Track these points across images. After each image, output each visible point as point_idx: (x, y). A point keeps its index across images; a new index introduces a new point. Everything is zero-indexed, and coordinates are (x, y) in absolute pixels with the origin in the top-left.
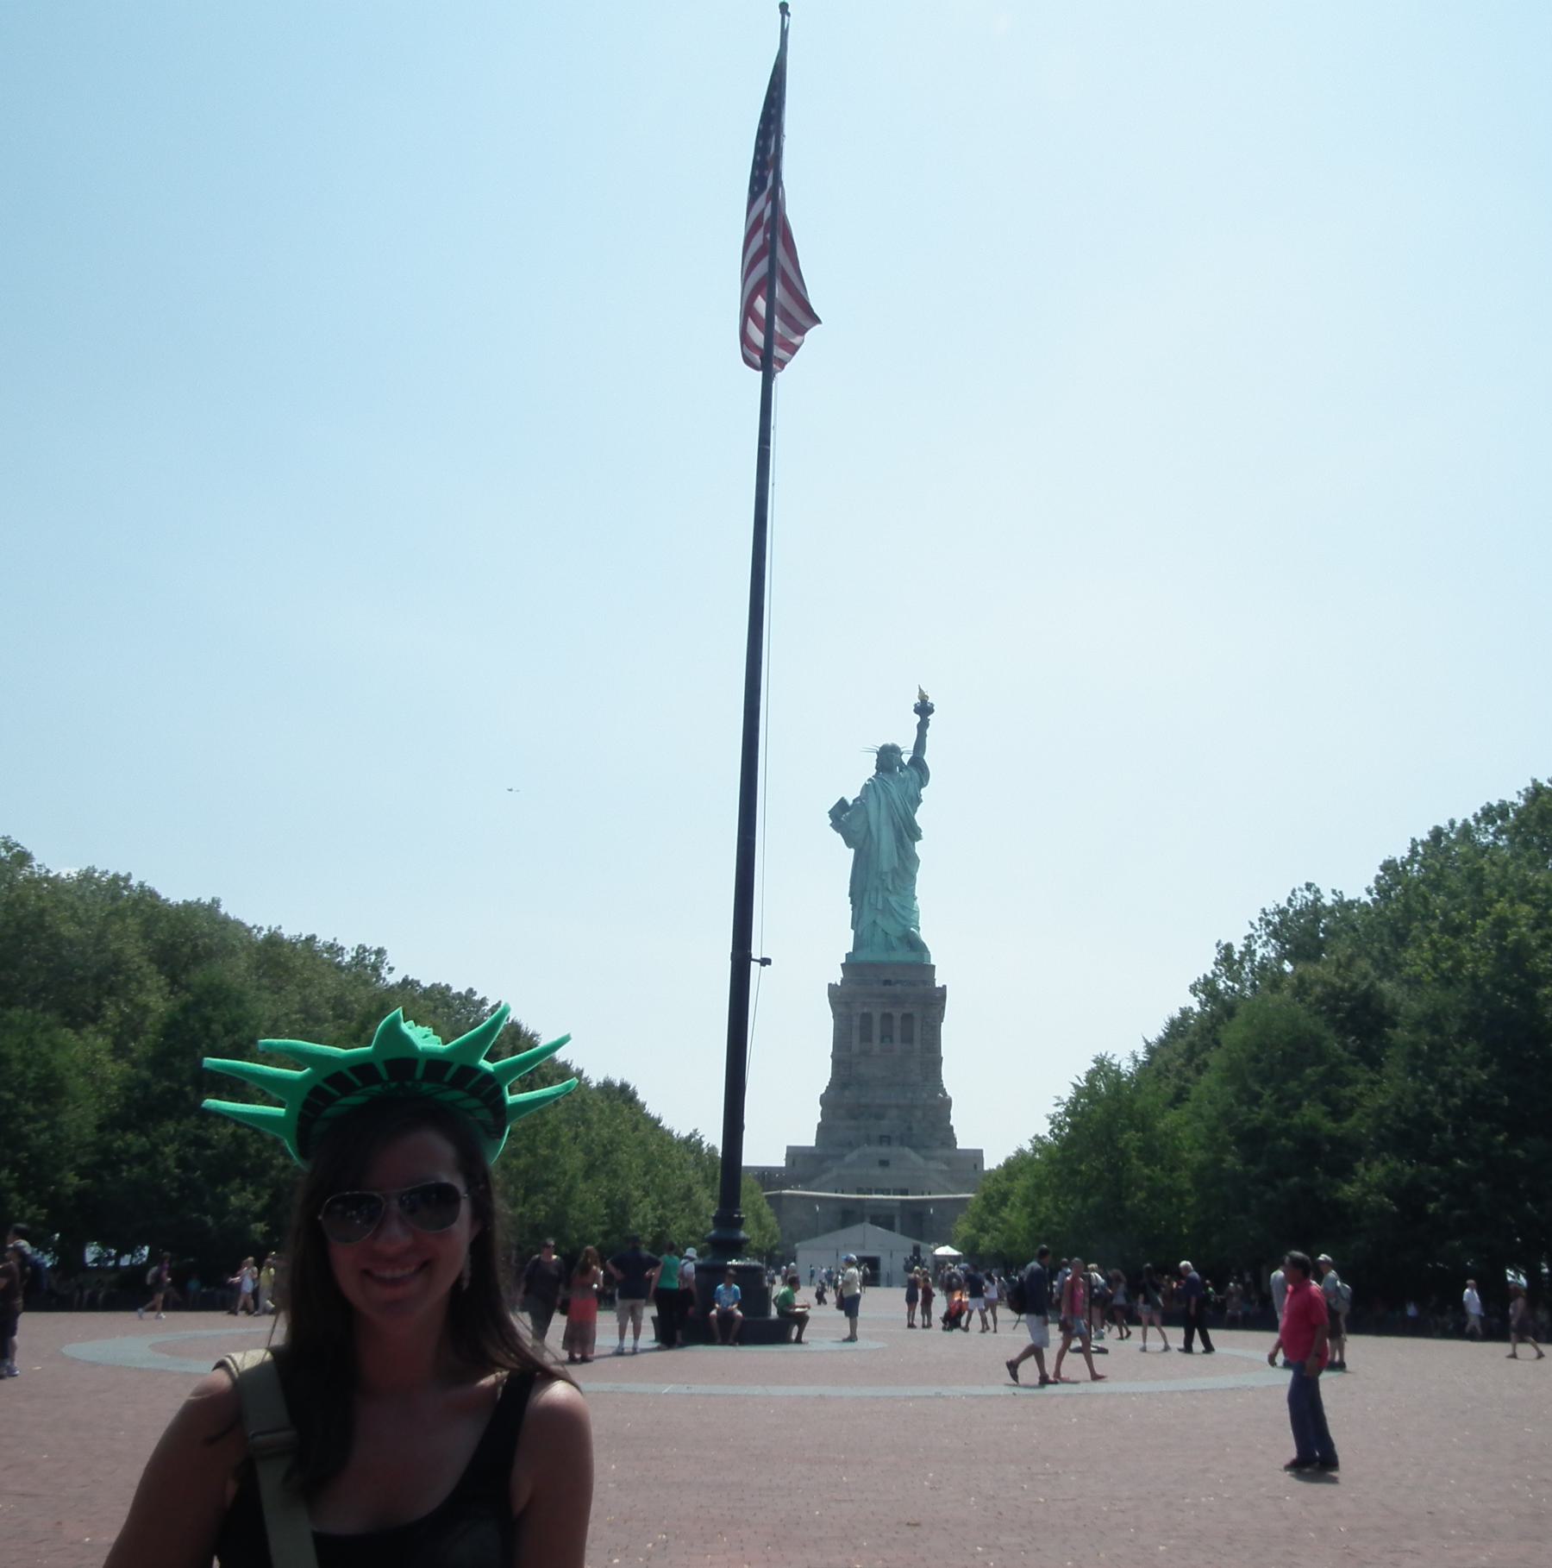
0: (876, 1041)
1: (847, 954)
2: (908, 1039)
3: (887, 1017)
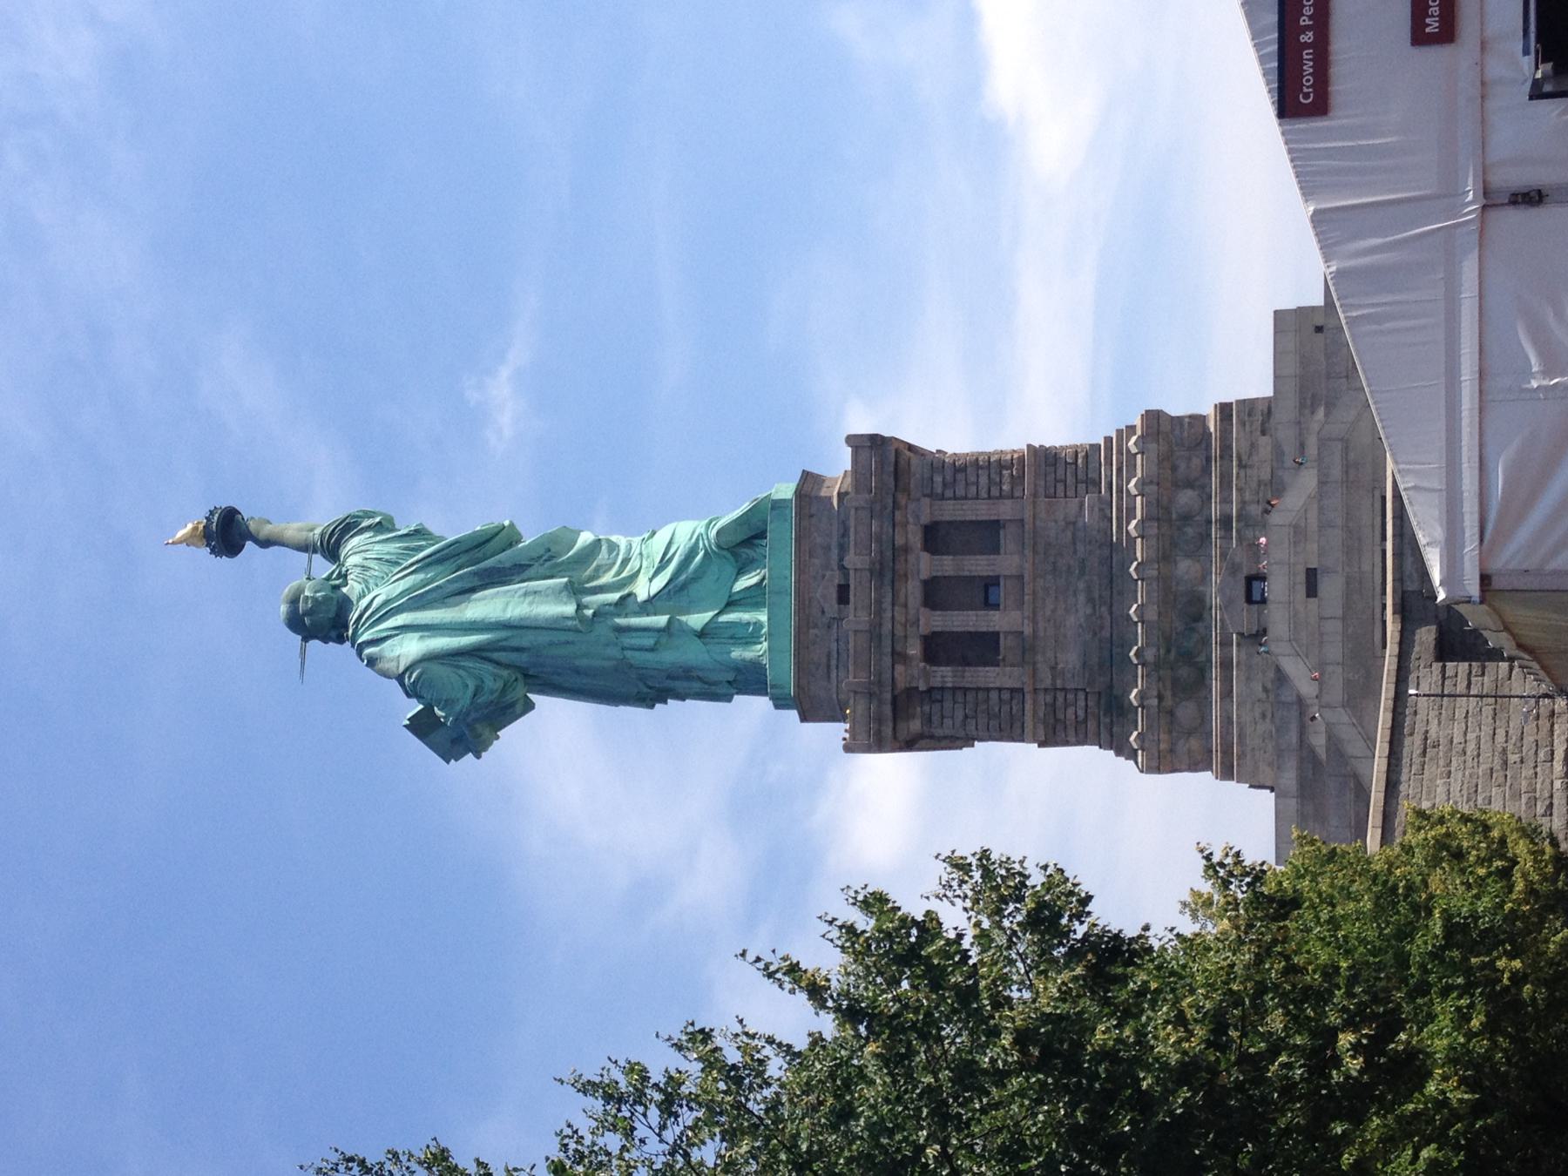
0: (996, 621)
1: (777, 707)
2: (987, 535)
3: (935, 593)
